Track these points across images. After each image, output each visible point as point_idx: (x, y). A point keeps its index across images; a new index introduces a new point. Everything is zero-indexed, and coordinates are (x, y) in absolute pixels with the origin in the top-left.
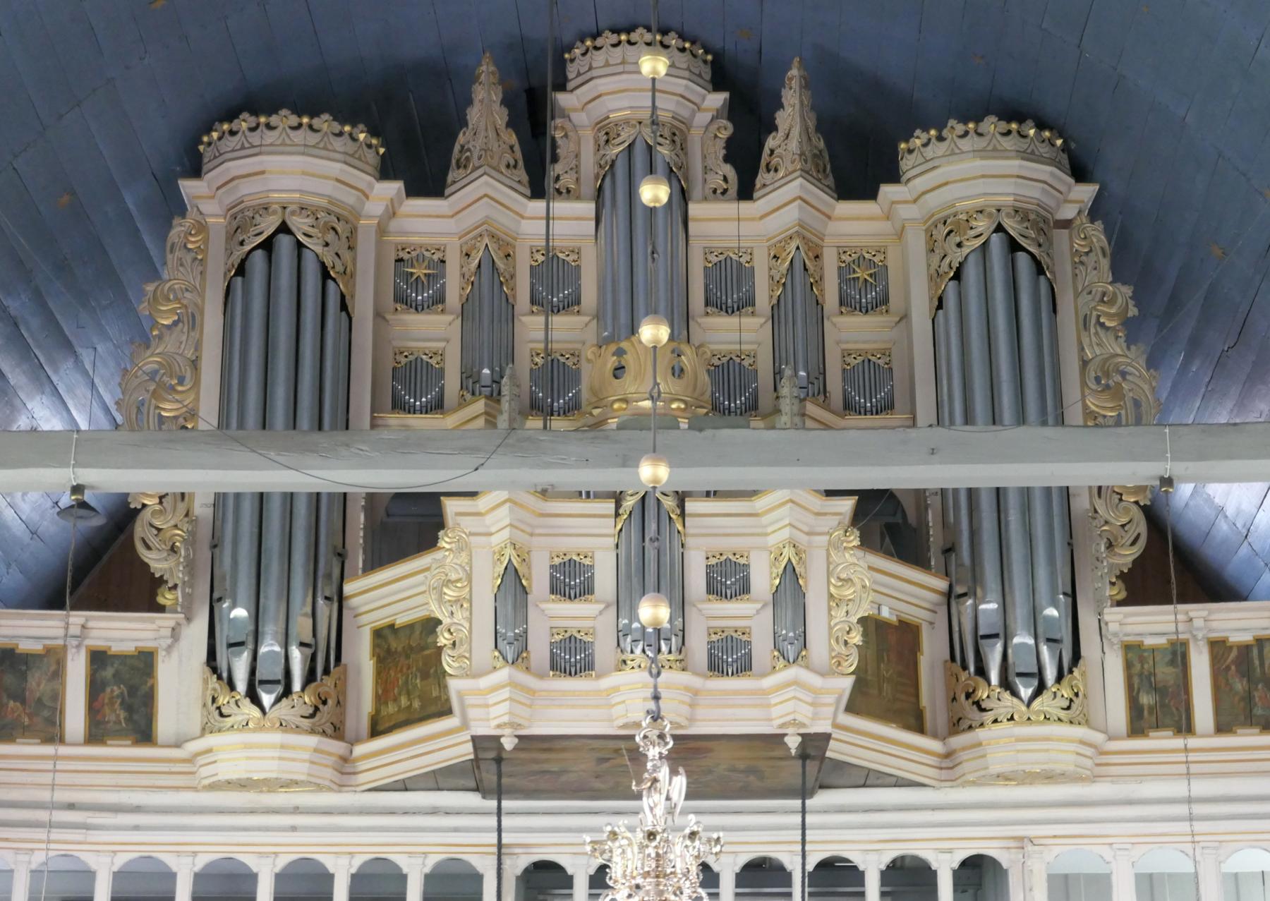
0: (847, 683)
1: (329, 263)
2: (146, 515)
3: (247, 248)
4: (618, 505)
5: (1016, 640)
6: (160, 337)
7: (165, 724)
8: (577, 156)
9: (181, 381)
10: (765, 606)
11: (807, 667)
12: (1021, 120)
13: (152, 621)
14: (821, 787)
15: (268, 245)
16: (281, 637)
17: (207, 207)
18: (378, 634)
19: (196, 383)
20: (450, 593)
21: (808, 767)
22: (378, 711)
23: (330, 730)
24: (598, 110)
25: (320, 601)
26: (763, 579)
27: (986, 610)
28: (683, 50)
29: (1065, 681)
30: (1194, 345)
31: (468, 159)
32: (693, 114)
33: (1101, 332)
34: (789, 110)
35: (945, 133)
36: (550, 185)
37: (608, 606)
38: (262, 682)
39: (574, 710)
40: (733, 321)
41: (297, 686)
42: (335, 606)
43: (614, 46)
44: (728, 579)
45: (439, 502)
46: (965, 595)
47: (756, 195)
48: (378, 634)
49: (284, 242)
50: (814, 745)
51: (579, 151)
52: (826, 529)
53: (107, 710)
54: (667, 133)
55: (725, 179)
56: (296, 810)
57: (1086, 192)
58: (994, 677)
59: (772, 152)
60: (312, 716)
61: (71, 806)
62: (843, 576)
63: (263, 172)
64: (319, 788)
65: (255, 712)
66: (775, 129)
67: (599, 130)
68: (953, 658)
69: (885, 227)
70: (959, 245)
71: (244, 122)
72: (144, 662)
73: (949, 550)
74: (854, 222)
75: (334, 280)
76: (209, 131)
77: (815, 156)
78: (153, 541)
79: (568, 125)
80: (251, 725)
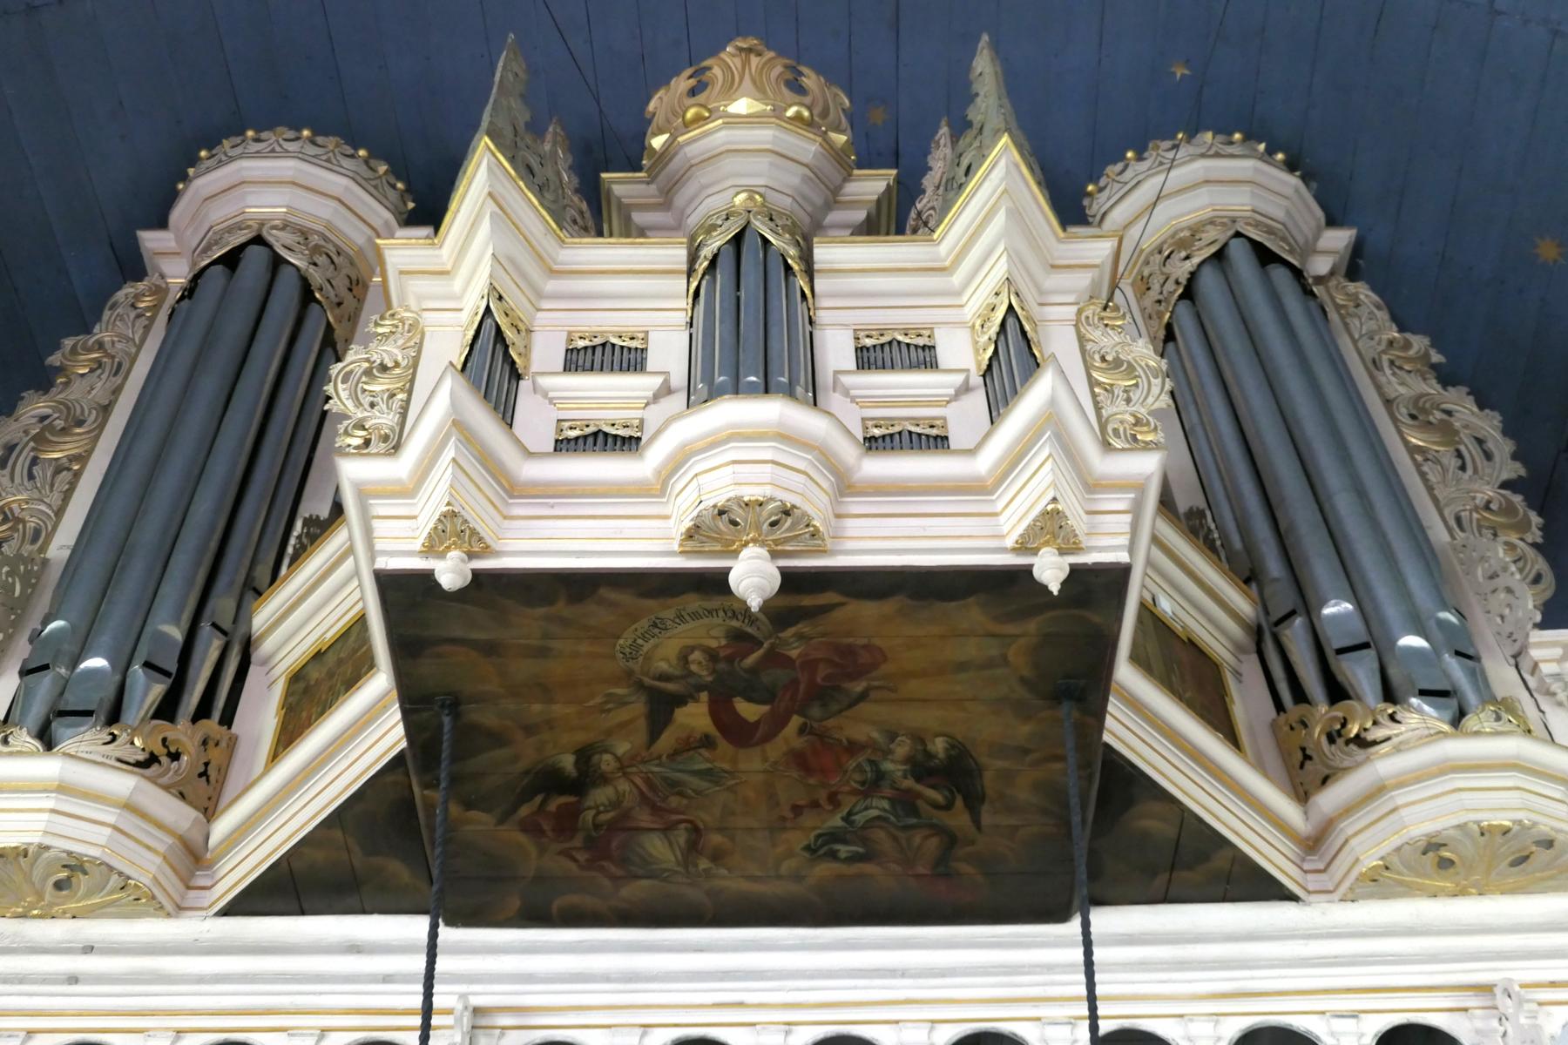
6: (67, 384)
19: (102, 427)
27: (1334, 617)
49: (255, 254)
52: (1071, 299)
75: (319, 302)
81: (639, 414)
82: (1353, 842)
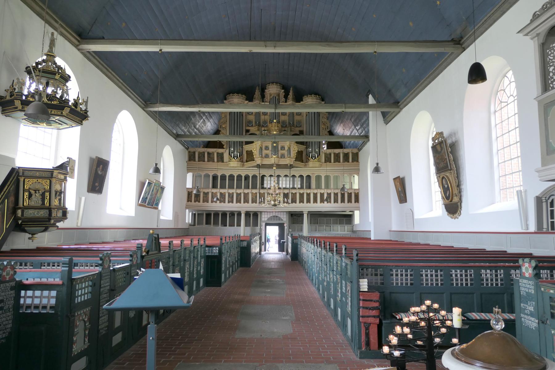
7: (225, 161)
26: (286, 148)
30: (335, 118)
39: (267, 162)
50: (291, 165)
71: (231, 95)
72: (222, 154)
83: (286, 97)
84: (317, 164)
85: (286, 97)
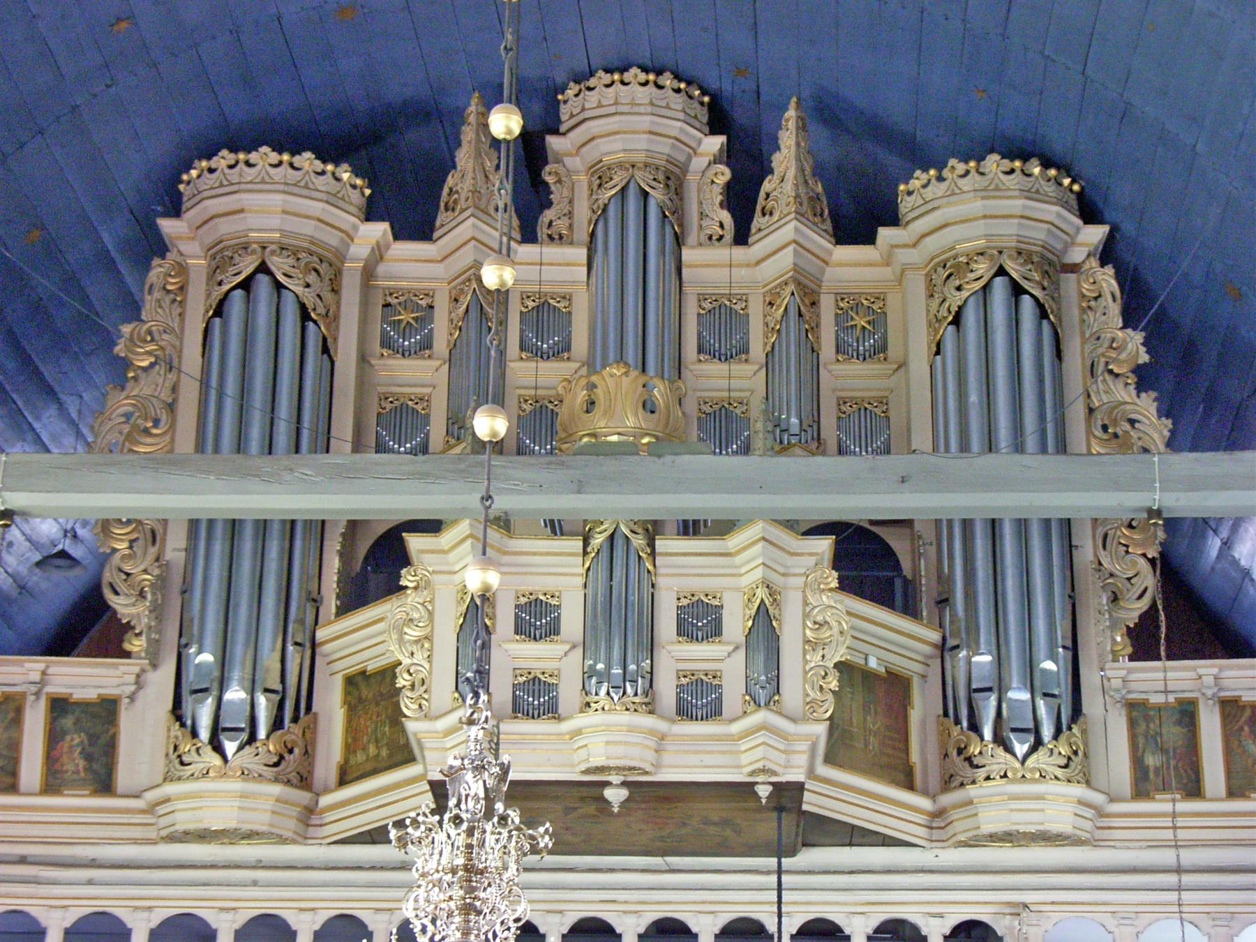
0: (821, 729)
1: (310, 306)
2: (116, 559)
3: (226, 288)
4: (586, 543)
5: (1011, 694)
8: (571, 202)
9: (156, 422)
10: (737, 648)
11: (780, 714)
12: (1025, 158)
13: (115, 666)
14: (805, 845)
15: (246, 285)
16: (248, 684)
17: (185, 247)
18: (350, 681)
19: (172, 427)
20: (412, 633)
21: (782, 820)
22: (346, 761)
23: (293, 777)
24: (592, 153)
25: (290, 648)
27: (978, 663)
28: (678, 91)
29: (1063, 738)
31: (456, 202)
32: (689, 159)
33: (1107, 376)
34: (784, 151)
35: (946, 173)
36: (542, 232)
37: (574, 647)
38: (225, 729)
40: (723, 368)
41: (262, 733)
42: (308, 653)
43: (608, 86)
44: (700, 620)
45: (402, 540)
46: (957, 647)
47: (750, 240)
48: (350, 681)
51: (573, 198)
52: (803, 571)
53: (65, 759)
54: (661, 177)
55: (722, 226)
56: (259, 865)
57: (1095, 234)
58: (988, 733)
59: (768, 195)
60: (276, 765)
61: (23, 860)
62: (819, 619)
63: (242, 211)
64: (283, 840)
65: (216, 760)
66: (771, 171)
67: (592, 175)
68: (946, 714)
69: (886, 273)
70: (959, 288)
71: (224, 158)
72: (107, 709)
73: (943, 602)
74: (850, 265)
75: (315, 322)
76: (187, 169)
77: (811, 199)
78: (121, 587)
79: (562, 171)
80: (212, 774)
81: (555, 664)
82: (955, 824)
83: (743, 202)
84: (1058, 803)
85: (743, 202)
